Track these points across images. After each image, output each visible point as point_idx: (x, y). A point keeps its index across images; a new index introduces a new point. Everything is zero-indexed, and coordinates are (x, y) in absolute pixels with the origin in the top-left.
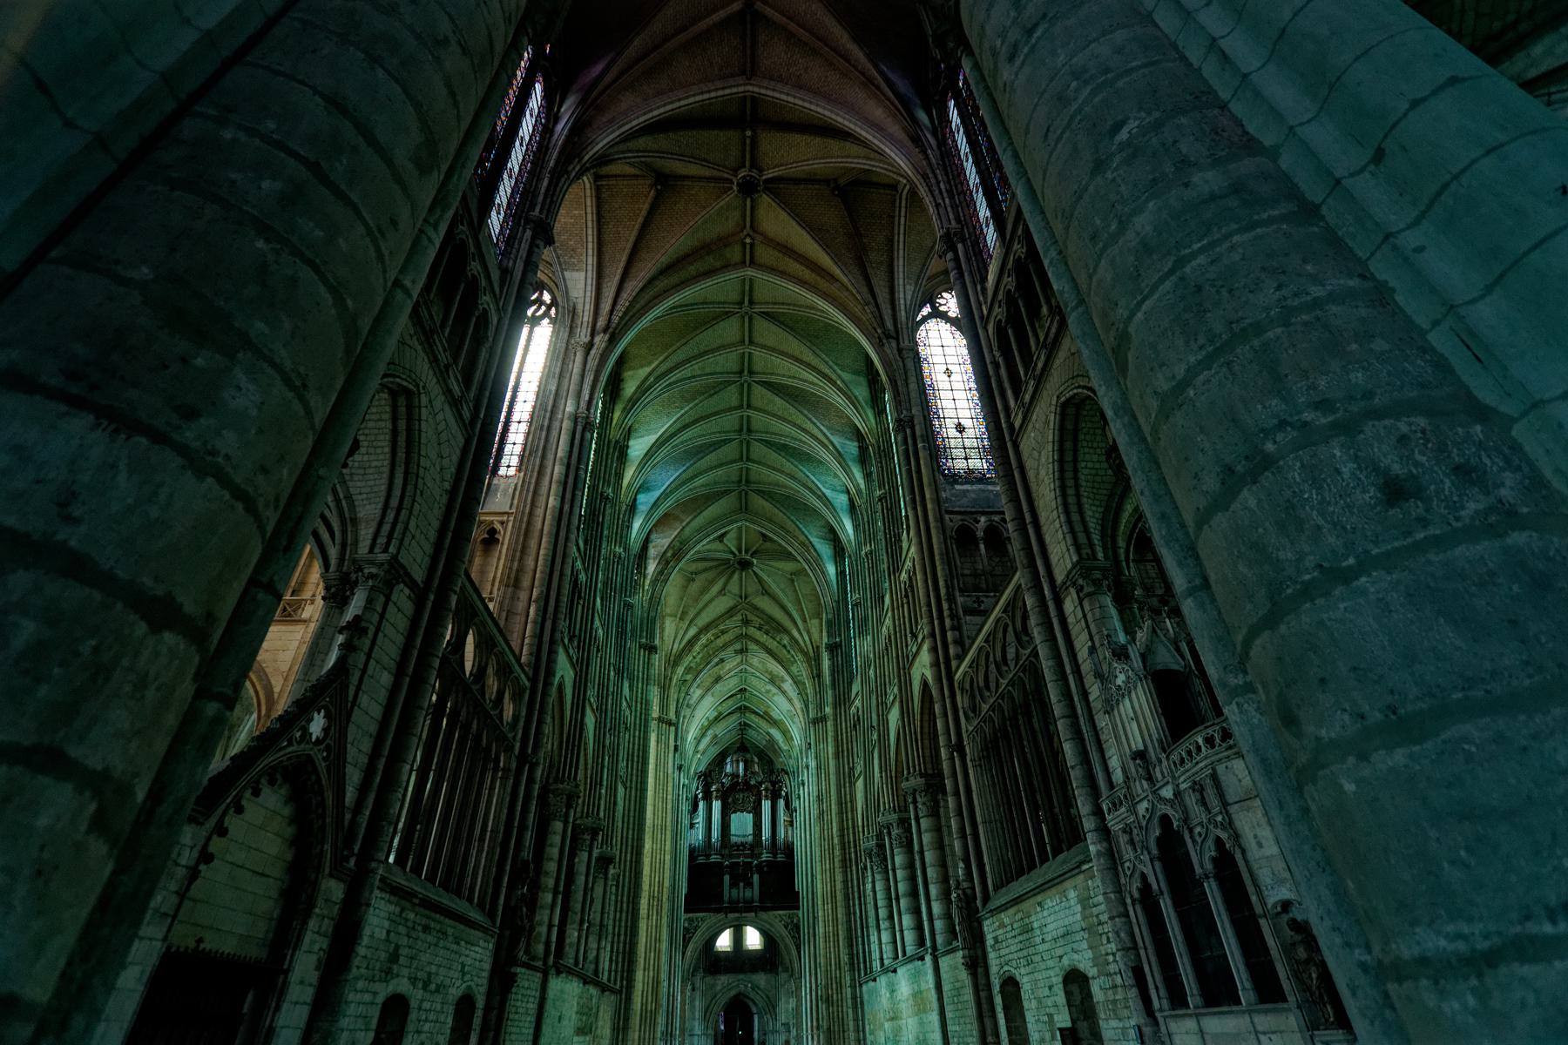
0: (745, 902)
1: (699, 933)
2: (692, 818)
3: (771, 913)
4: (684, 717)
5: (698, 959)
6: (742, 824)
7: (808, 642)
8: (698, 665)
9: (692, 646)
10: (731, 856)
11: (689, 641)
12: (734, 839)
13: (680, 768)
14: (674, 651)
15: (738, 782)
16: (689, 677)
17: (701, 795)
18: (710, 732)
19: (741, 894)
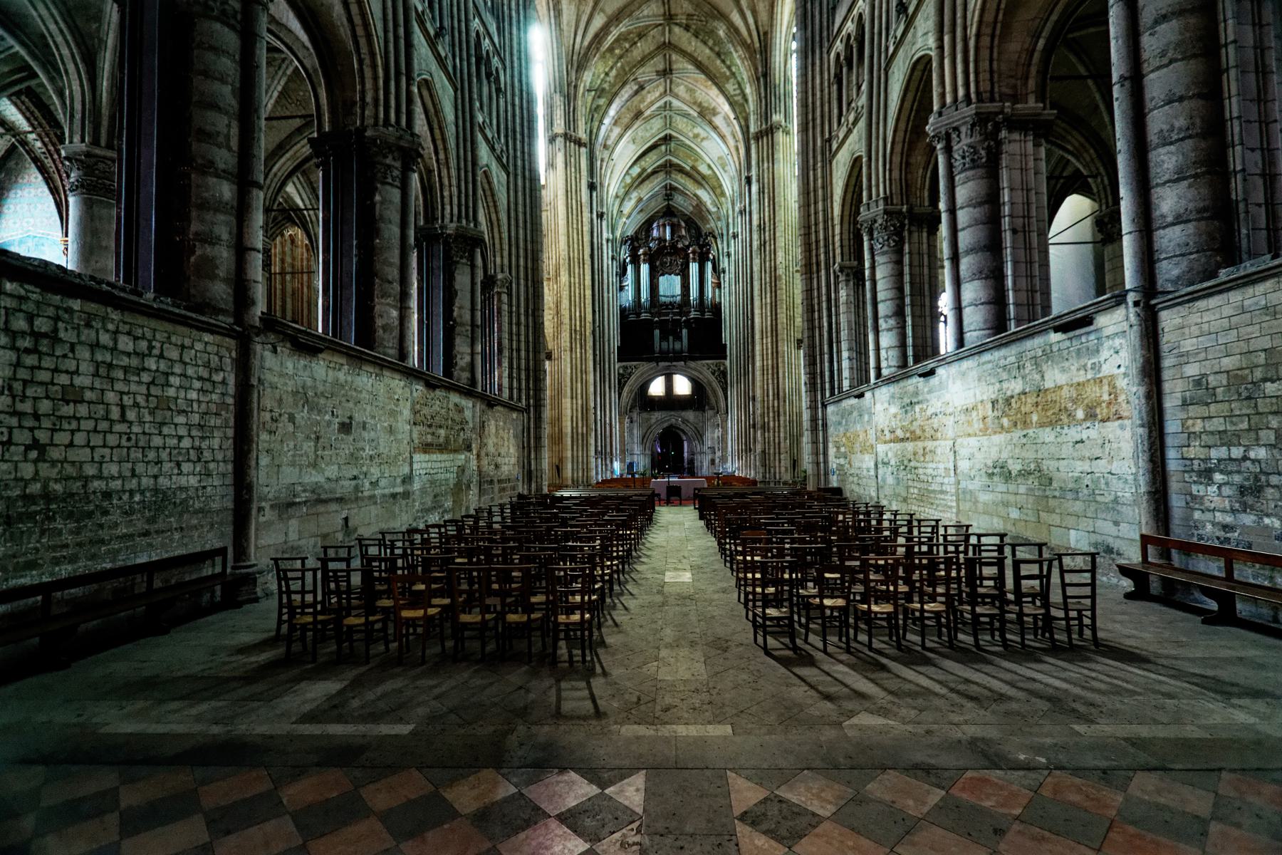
0: (674, 351)
1: (633, 378)
2: (621, 282)
3: (699, 362)
4: (602, 160)
5: (634, 400)
6: (670, 286)
7: (753, 27)
8: (612, 85)
9: (600, 43)
10: (660, 314)
11: (596, 36)
12: (663, 299)
13: (601, 216)
14: (577, 46)
15: (665, 247)
16: (602, 101)
17: (628, 260)
18: (634, 196)
19: (671, 347)
